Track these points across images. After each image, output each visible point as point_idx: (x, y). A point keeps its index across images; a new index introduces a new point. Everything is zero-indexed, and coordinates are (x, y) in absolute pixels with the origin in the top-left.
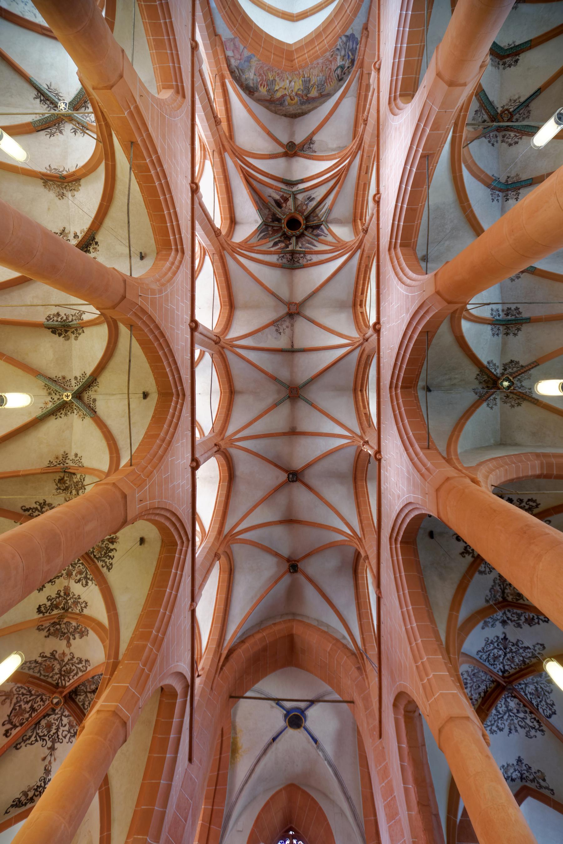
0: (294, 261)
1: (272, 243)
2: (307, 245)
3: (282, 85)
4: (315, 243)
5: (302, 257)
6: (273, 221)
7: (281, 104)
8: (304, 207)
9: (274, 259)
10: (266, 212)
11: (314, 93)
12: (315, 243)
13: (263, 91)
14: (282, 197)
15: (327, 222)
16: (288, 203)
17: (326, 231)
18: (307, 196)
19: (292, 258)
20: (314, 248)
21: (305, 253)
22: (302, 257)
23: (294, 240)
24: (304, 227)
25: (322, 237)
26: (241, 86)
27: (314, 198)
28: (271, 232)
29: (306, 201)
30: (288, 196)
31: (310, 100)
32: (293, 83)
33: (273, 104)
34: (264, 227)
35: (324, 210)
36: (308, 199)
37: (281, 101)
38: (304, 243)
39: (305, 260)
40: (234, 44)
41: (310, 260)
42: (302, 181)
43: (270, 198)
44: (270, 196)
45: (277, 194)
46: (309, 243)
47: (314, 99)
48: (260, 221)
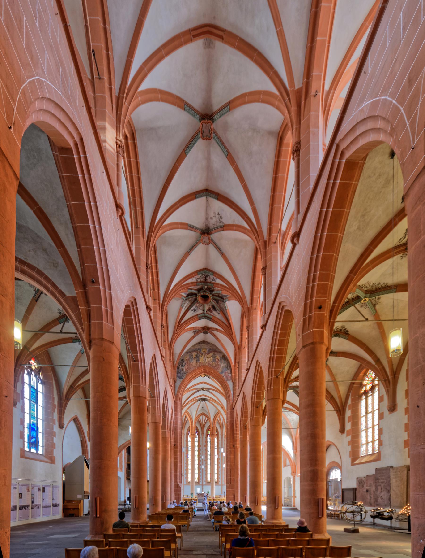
3: (209, 359)
7: (210, 349)
11: (194, 354)
13: (218, 357)
14: (211, 312)
26: (228, 360)
31: (196, 350)
32: (204, 360)
33: (214, 350)
37: (210, 351)
40: (227, 378)
47: (194, 351)
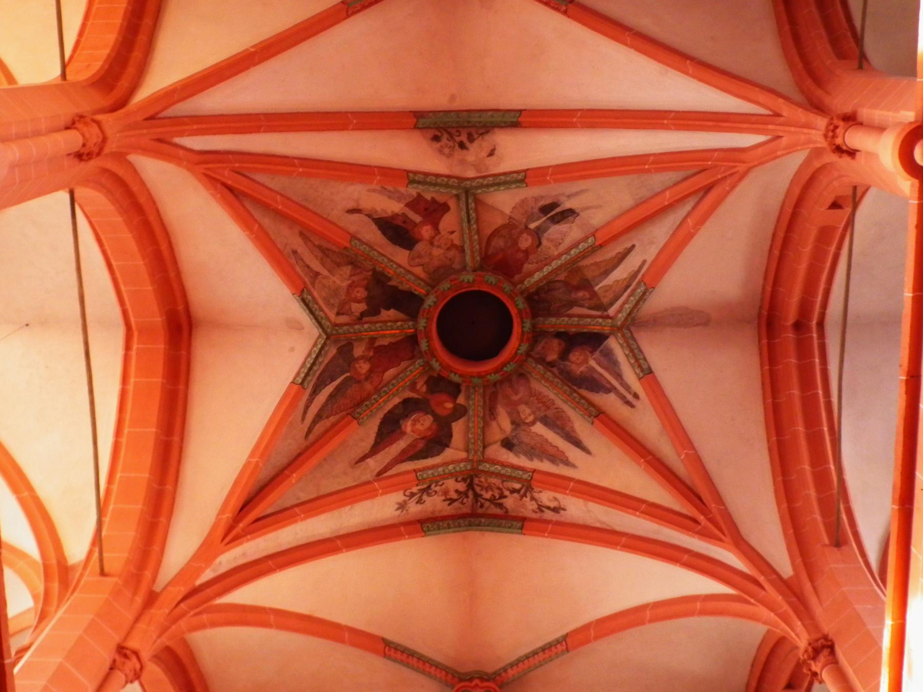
0: (477, 496)
1: (371, 427)
2: (539, 429)
4: (581, 426)
5: (513, 491)
6: (373, 310)
8: (525, 242)
9: (383, 508)
10: (340, 279)
12: (581, 426)
15: (632, 325)
16: (448, 222)
17: (630, 375)
18: (536, 200)
19: (471, 486)
20: (573, 453)
21: (528, 484)
22: (513, 491)
23: (473, 401)
24: (524, 348)
25: (609, 402)
27: (569, 214)
28: (364, 367)
29: (531, 218)
30: (441, 199)
34: (332, 351)
35: (620, 274)
36: (545, 210)
38: (526, 412)
39: (532, 506)
41: (556, 510)
42: (519, 120)
43: (356, 217)
44: (352, 211)
45: (391, 195)
46: (545, 421)
48: (312, 331)
